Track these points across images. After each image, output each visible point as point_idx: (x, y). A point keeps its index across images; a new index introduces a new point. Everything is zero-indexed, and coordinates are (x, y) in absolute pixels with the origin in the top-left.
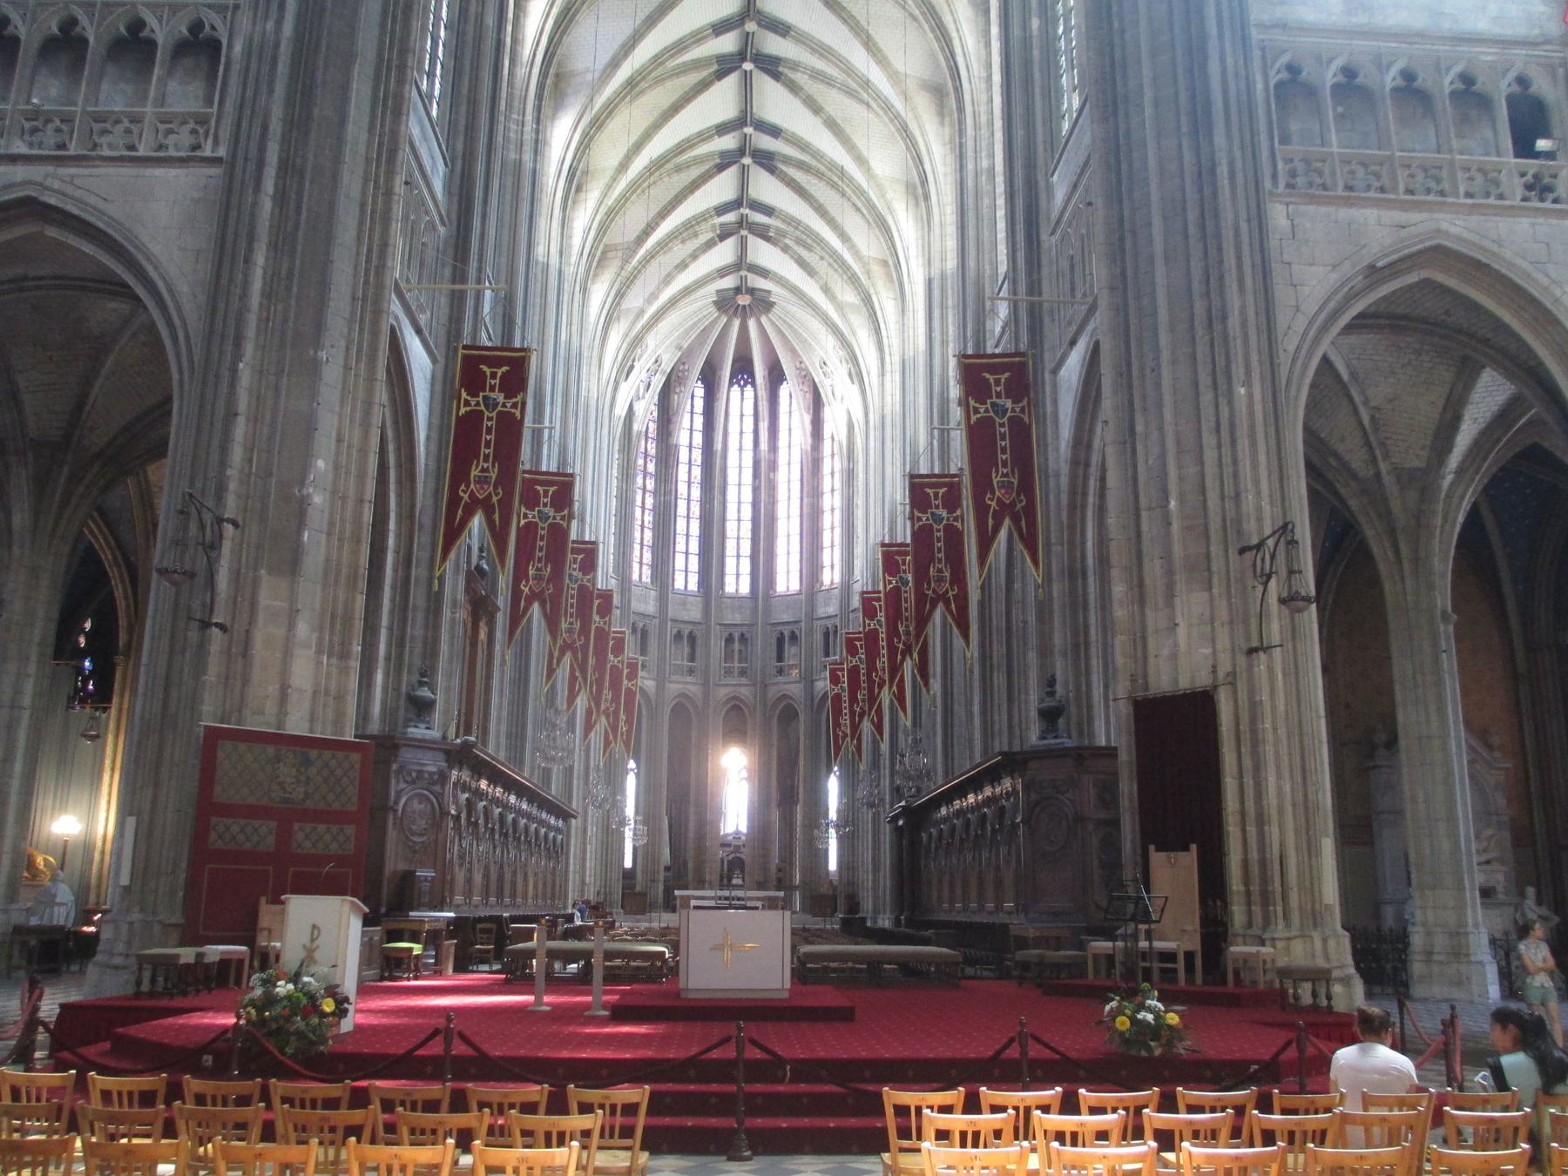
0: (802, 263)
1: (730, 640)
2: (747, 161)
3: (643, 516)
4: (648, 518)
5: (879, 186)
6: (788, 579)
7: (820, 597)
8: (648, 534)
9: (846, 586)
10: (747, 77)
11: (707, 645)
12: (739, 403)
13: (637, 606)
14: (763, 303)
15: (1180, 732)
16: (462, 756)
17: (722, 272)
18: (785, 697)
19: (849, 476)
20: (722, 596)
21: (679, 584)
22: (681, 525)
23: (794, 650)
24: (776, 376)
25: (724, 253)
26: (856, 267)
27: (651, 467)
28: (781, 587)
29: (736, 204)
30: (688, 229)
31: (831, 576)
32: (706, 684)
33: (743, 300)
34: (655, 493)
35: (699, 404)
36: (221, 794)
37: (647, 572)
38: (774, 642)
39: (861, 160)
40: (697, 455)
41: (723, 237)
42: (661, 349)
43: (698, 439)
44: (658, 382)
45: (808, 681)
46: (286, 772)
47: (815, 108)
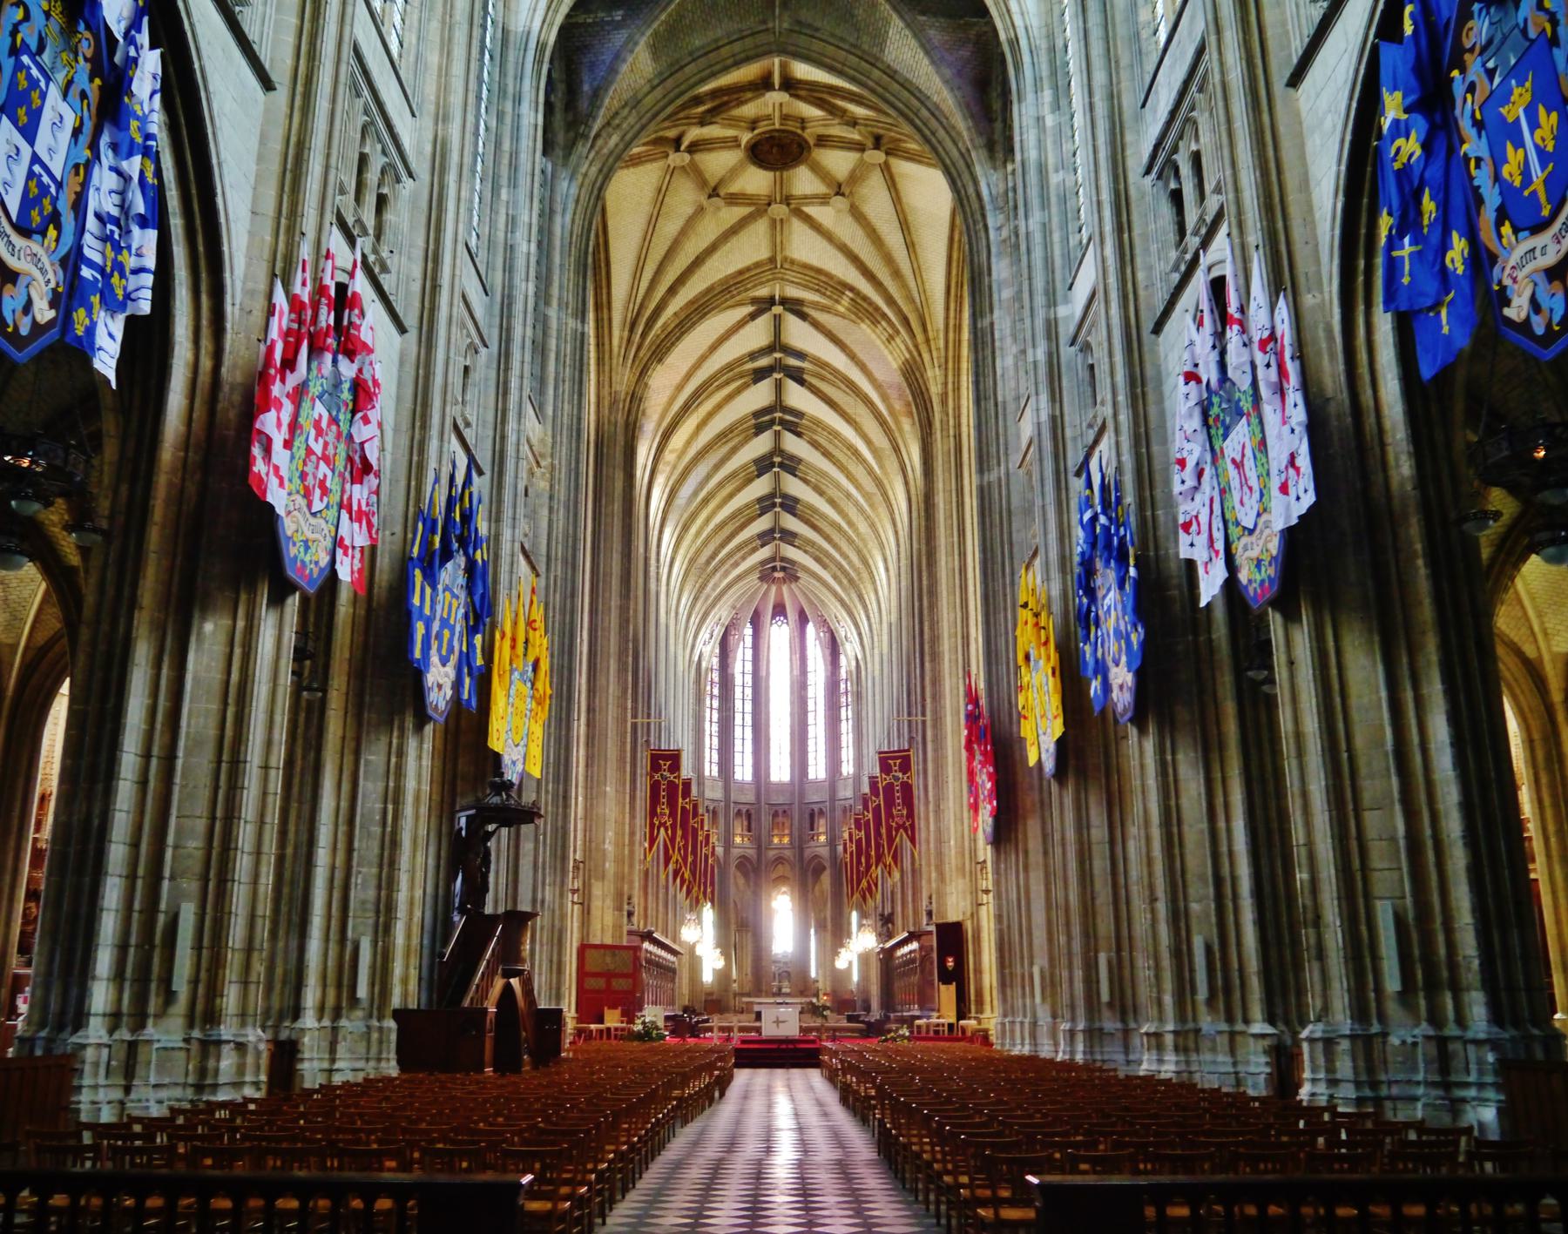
0: (817, 560)
1: (775, 815)
2: (778, 509)
3: (711, 729)
4: (715, 728)
5: (863, 540)
6: (817, 770)
7: (840, 785)
8: (715, 741)
9: (857, 778)
10: (777, 475)
11: (759, 819)
12: (779, 635)
13: (709, 794)
14: (790, 572)
15: (952, 938)
16: (648, 937)
17: (763, 563)
18: (816, 856)
19: (858, 696)
20: (768, 783)
21: (738, 776)
22: (738, 732)
23: (822, 822)
24: (803, 619)
25: (765, 553)
26: (853, 574)
27: (716, 691)
28: (811, 776)
29: (770, 349)
30: (739, 548)
31: (847, 769)
32: (759, 848)
33: (779, 571)
34: (720, 710)
35: (749, 640)
36: (589, 967)
37: (715, 769)
38: (807, 816)
39: (850, 523)
40: (749, 679)
41: (763, 546)
42: (723, 613)
43: (749, 667)
44: (718, 632)
45: (832, 843)
46: (608, 959)
47: (821, 493)
